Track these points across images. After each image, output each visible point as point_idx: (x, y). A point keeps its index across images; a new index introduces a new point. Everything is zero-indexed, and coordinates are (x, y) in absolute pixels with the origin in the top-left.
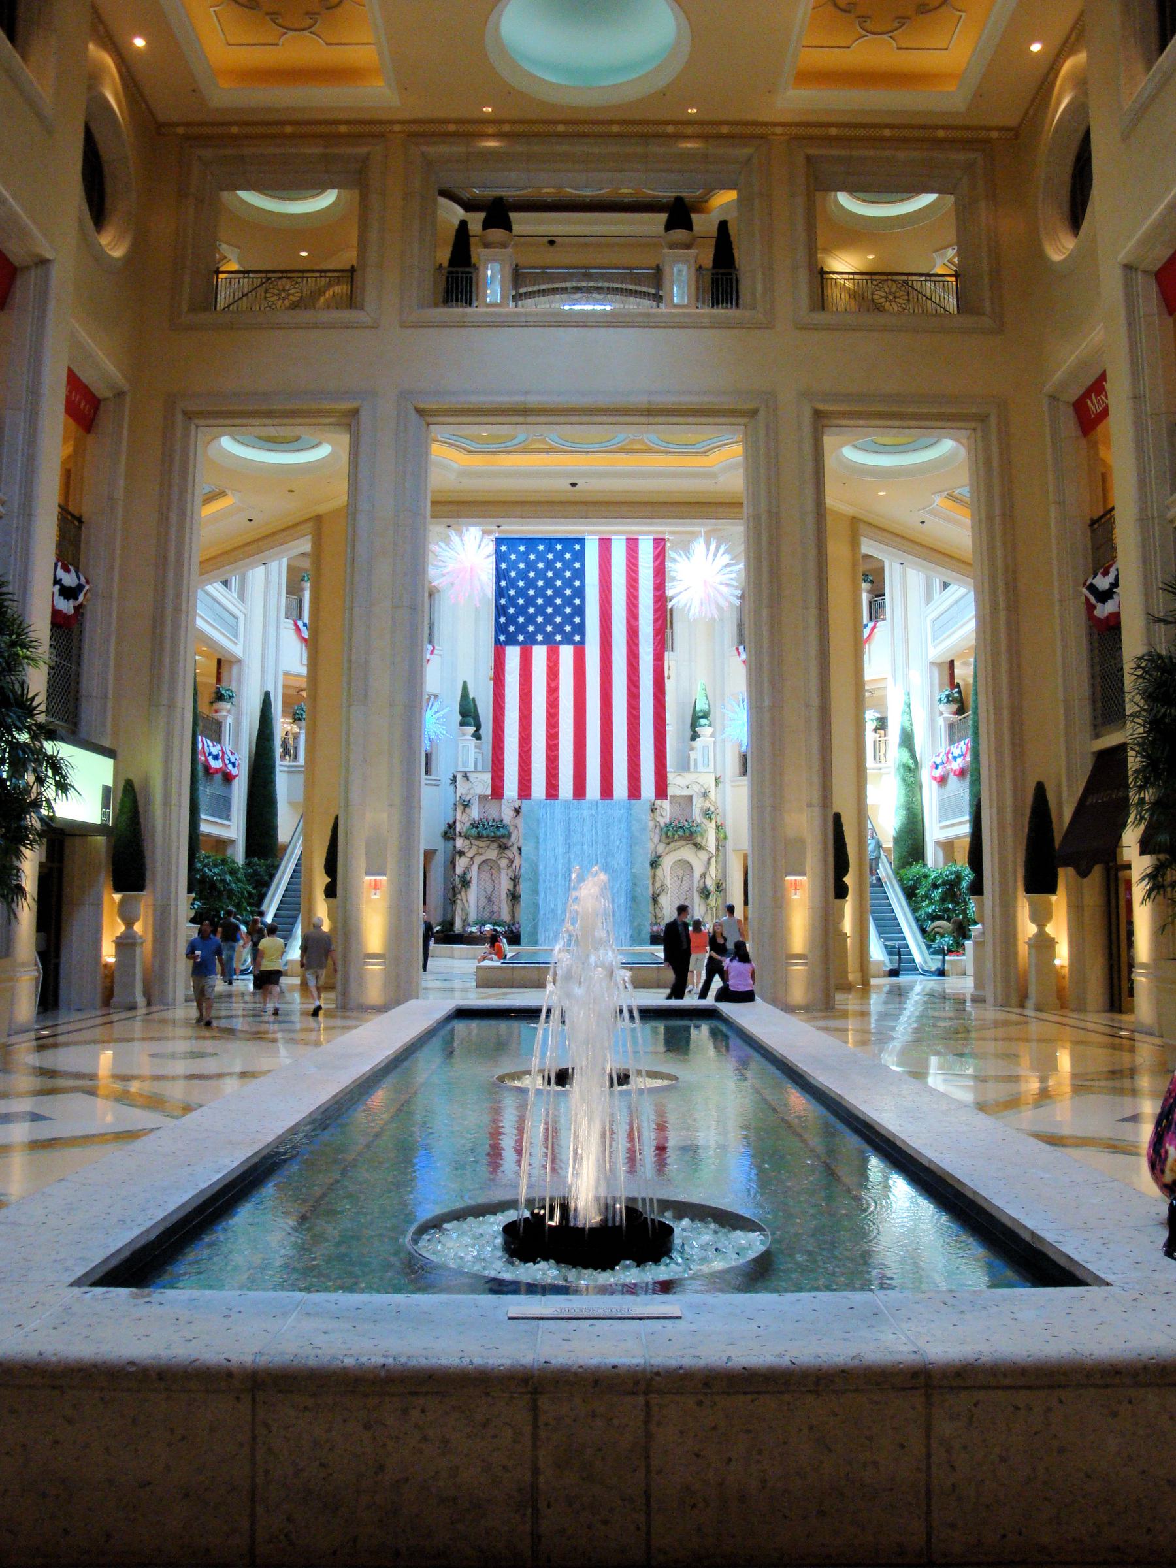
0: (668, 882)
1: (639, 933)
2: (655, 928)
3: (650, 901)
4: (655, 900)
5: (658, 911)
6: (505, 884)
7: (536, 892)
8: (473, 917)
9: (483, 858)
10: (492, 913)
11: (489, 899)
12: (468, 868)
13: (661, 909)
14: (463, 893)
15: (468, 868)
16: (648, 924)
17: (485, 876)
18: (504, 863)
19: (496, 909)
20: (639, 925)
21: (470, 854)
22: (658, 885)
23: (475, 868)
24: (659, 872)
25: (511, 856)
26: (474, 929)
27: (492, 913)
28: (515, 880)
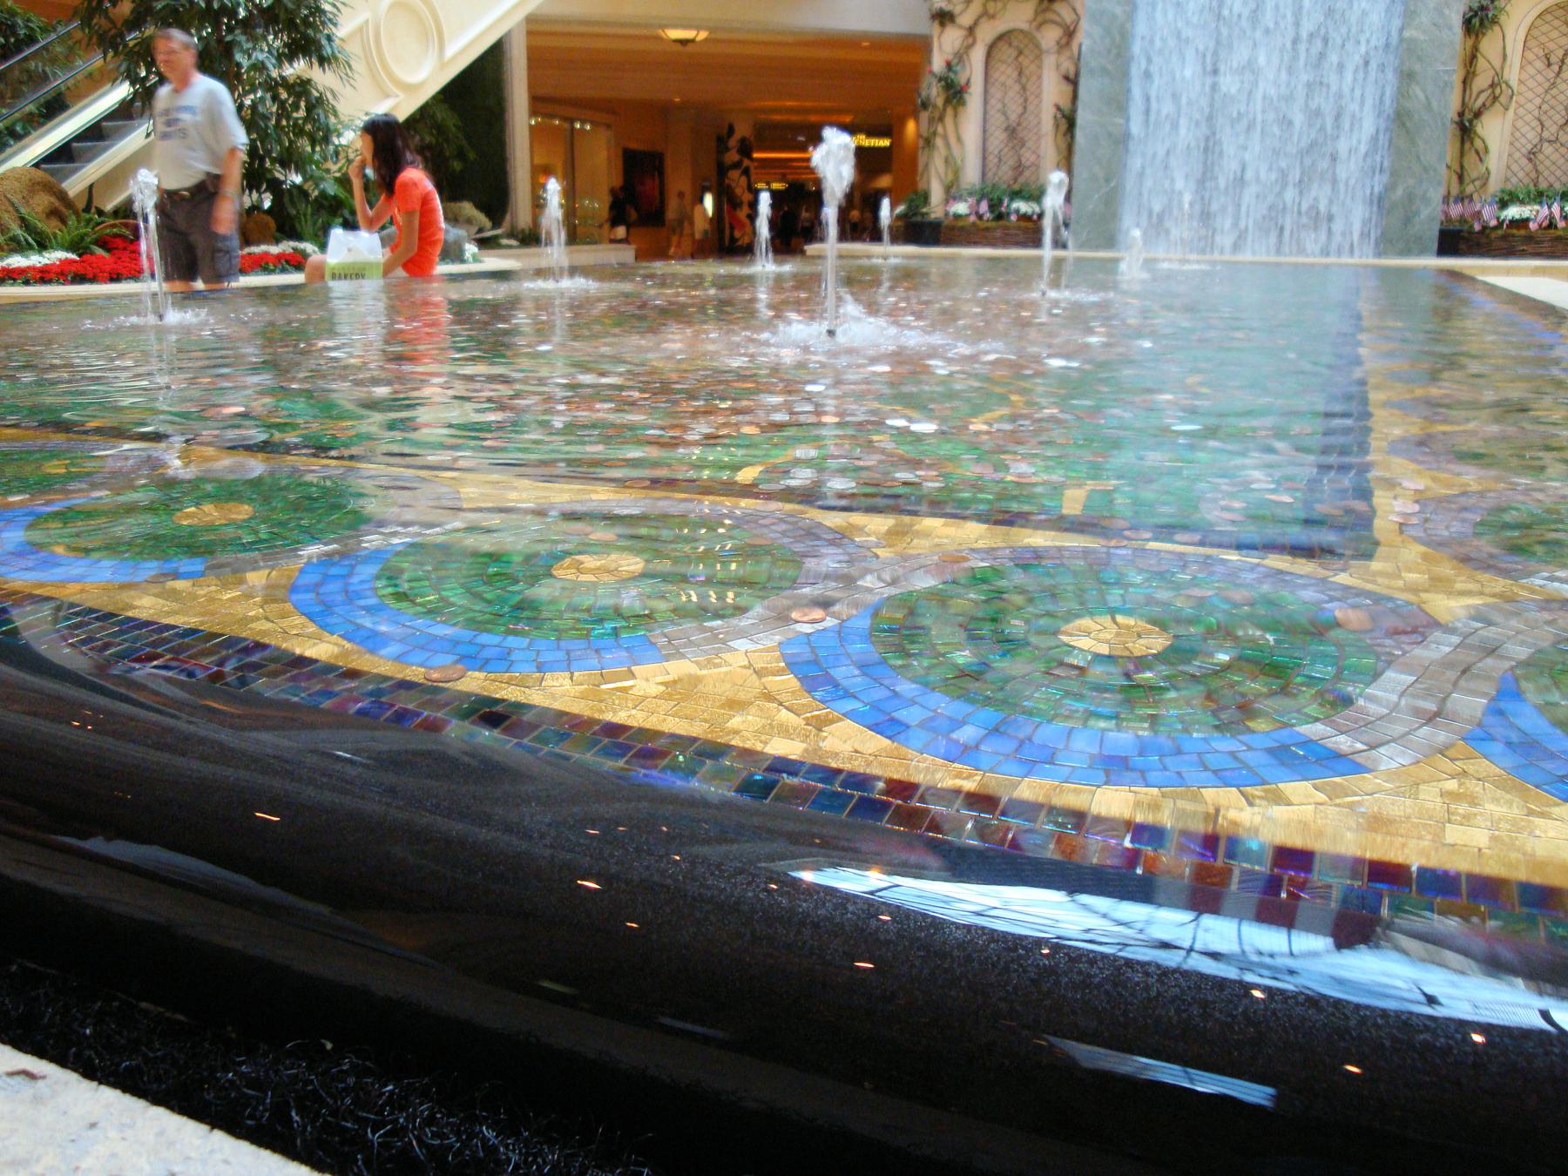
0: (1513, 75)
1: (1407, 221)
2: (1456, 210)
3: (1452, 130)
4: (1465, 129)
5: (1471, 158)
6: (1051, 91)
7: (1119, 103)
8: (971, 175)
9: (1000, 26)
10: (1019, 168)
11: (1012, 132)
12: (961, 56)
13: (1481, 155)
14: (949, 119)
15: (961, 56)
16: (1436, 195)
17: (1005, 73)
18: (1050, 37)
19: (1028, 157)
20: (1410, 197)
21: (966, 19)
22: (1481, 82)
23: (978, 55)
24: (1489, 45)
25: (1068, 17)
26: (961, 208)
27: (1019, 168)
28: (1073, 81)
